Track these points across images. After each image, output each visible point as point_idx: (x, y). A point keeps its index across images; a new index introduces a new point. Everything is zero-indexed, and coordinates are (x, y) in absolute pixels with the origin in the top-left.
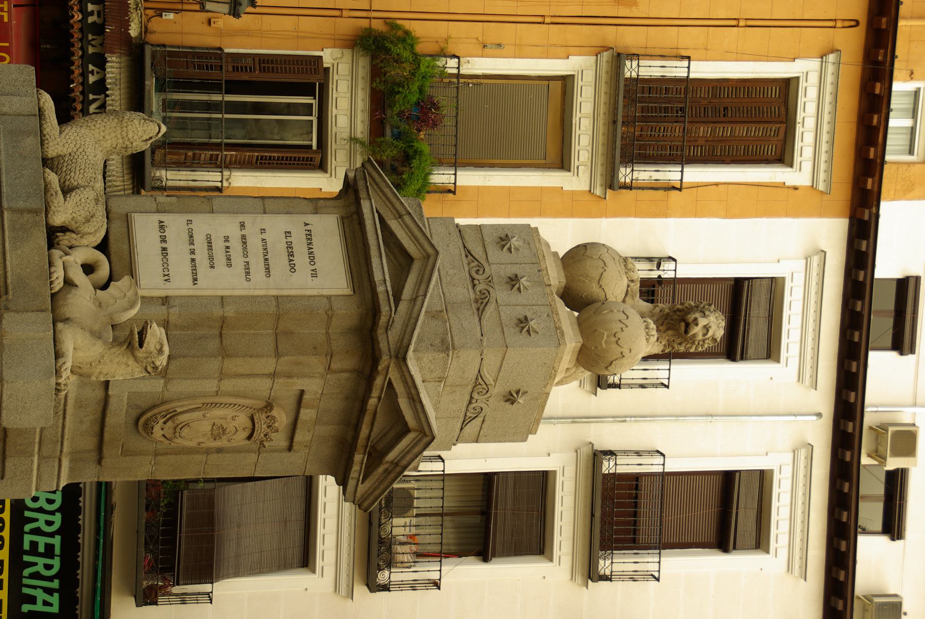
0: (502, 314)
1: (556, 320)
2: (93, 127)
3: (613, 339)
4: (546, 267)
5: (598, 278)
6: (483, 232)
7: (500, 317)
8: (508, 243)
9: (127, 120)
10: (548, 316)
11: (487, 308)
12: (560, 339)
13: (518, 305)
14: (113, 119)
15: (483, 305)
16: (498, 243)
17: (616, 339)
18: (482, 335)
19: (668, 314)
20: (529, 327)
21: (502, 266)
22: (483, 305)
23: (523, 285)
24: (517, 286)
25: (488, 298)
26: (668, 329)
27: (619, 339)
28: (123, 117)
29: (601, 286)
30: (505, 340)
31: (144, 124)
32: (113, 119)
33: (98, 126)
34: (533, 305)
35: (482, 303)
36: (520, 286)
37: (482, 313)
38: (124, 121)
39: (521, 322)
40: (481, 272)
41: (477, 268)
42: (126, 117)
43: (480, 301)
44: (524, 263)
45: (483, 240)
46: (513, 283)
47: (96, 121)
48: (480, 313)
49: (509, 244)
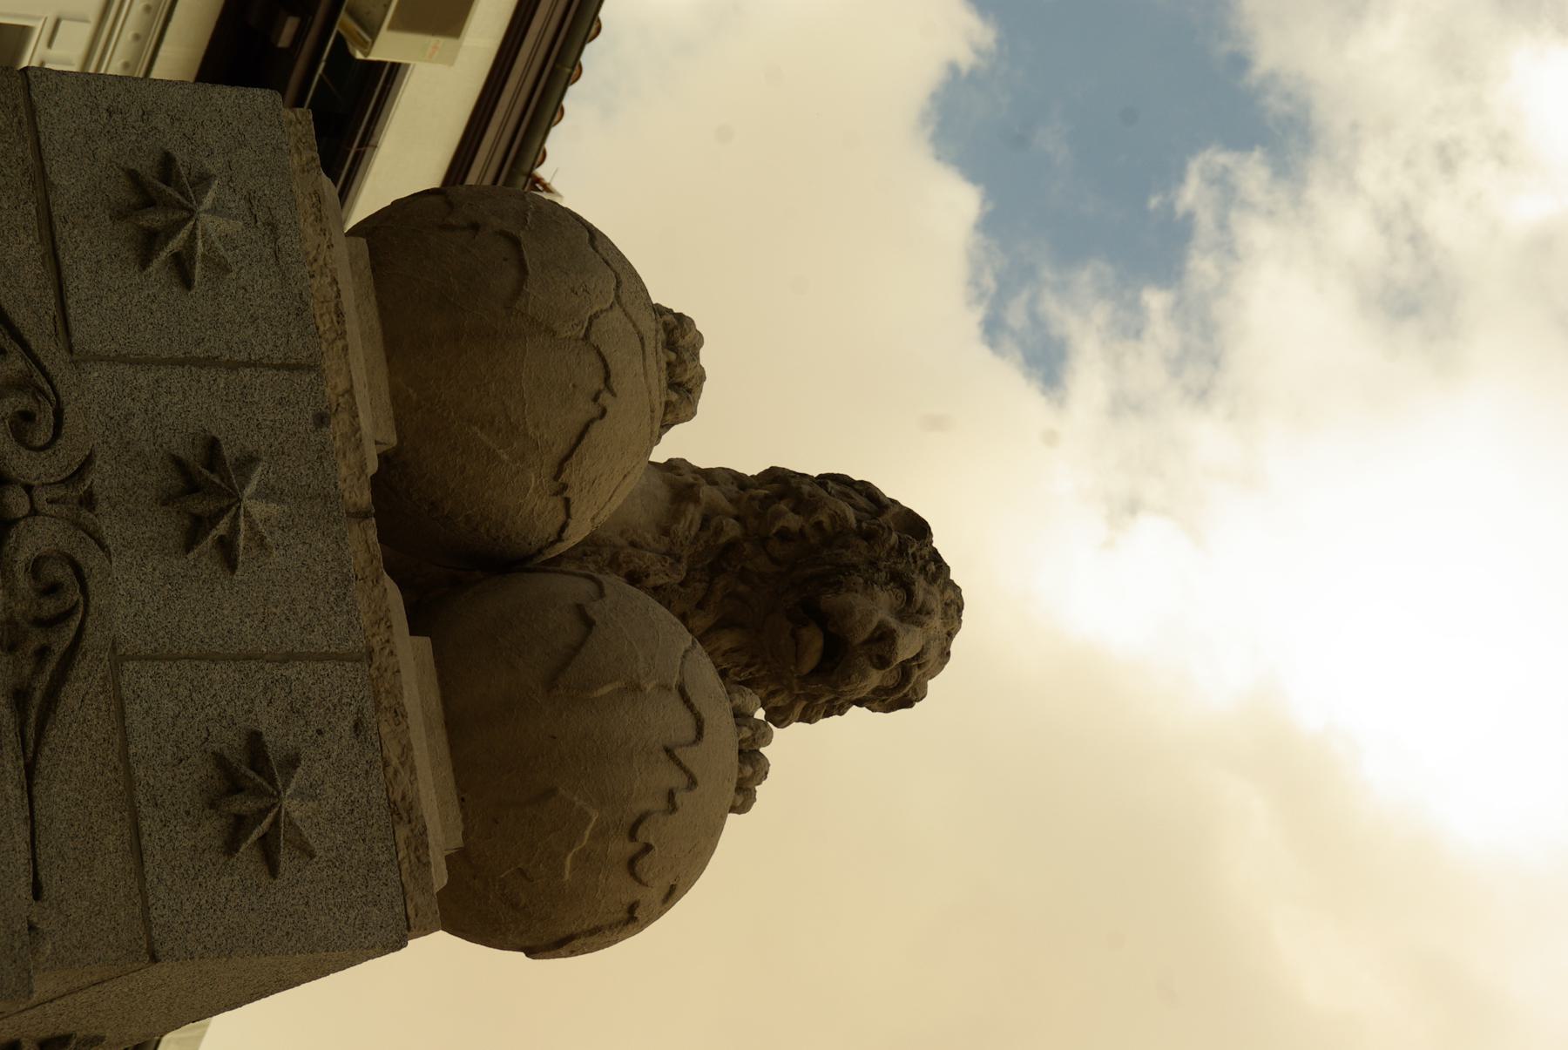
0: (134, 710)
1: (393, 752)
3: (621, 848)
4: (350, 391)
5: (560, 448)
6: (42, 122)
7: (125, 743)
8: (179, 225)
10: (357, 727)
11: (70, 697)
12: (410, 888)
13: (214, 658)
15: (50, 667)
16: (120, 215)
17: (632, 848)
18: (37, 891)
19: (732, 545)
20: (275, 823)
21: (144, 379)
22: (50, 667)
23: (252, 526)
24: (222, 528)
25: (74, 624)
26: (723, 624)
27: (648, 848)
29: (565, 487)
30: (146, 909)
34: (289, 658)
35: (42, 653)
36: (234, 530)
37: (37, 744)
39: (235, 787)
40: (42, 435)
41: (24, 402)
43: (36, 639)
44: (247, 364)
45: (41, 180)
46: (200, 506)
48: (31, 733)
49: (183, 234)
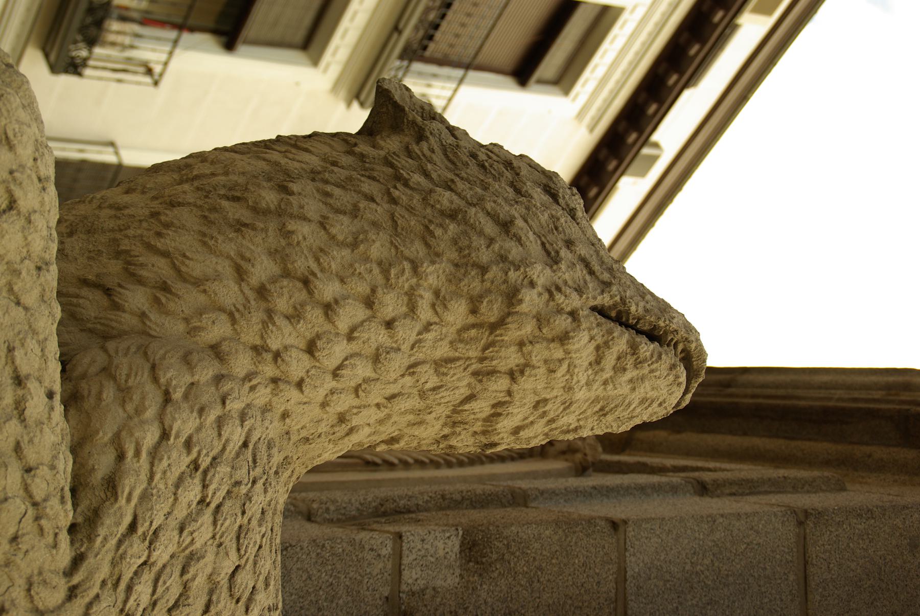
2: (297, 365)
9: (529, 328)
14: (440, 300)
28: (512, 297)
31: (619, 369)
32: (440, 300)
33: (338, 350)
38: (512, 333)
42: (531, 300)
47: (329, 309)
